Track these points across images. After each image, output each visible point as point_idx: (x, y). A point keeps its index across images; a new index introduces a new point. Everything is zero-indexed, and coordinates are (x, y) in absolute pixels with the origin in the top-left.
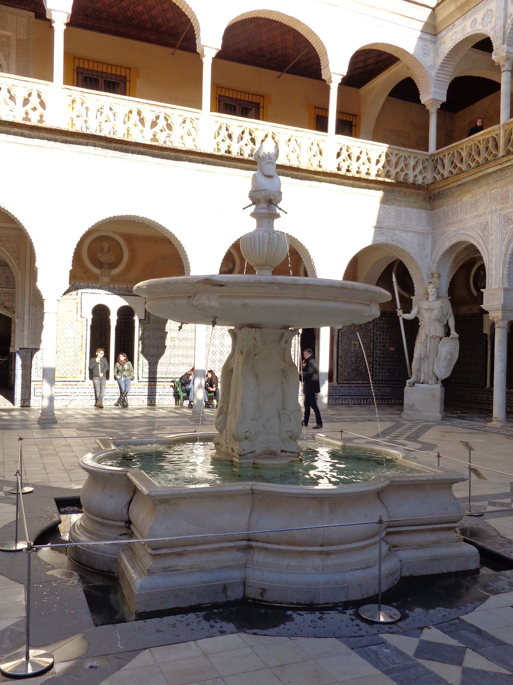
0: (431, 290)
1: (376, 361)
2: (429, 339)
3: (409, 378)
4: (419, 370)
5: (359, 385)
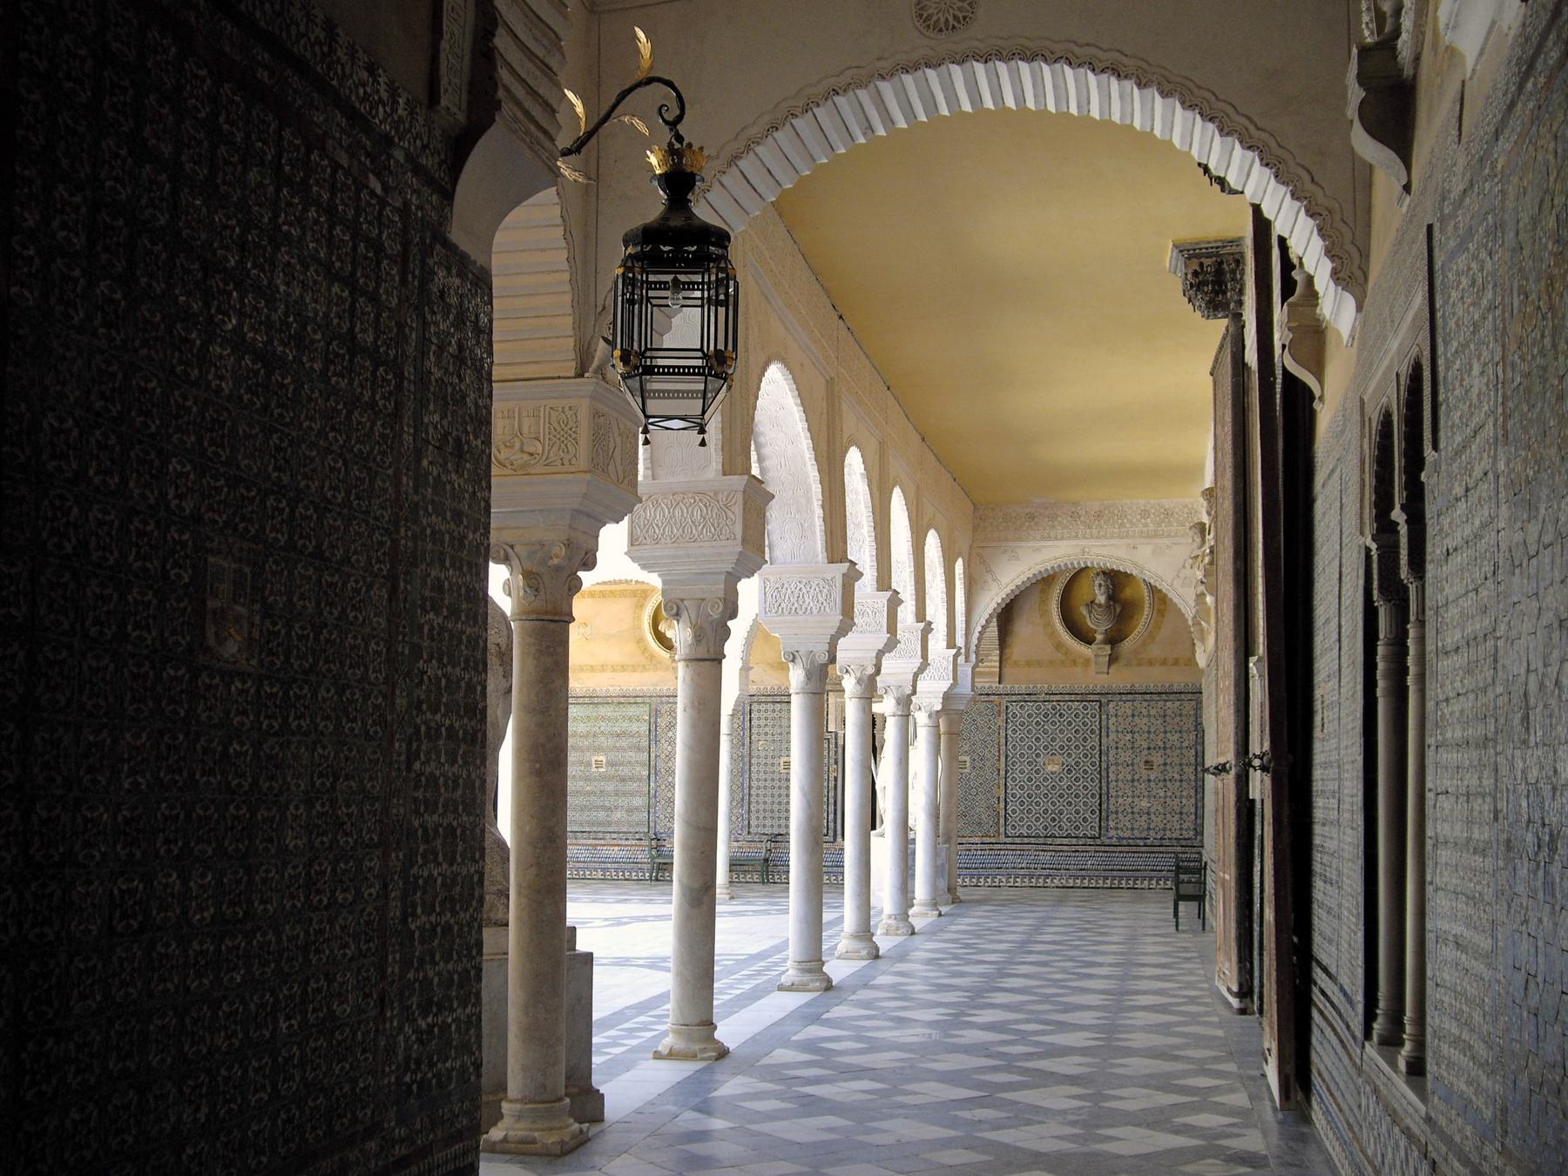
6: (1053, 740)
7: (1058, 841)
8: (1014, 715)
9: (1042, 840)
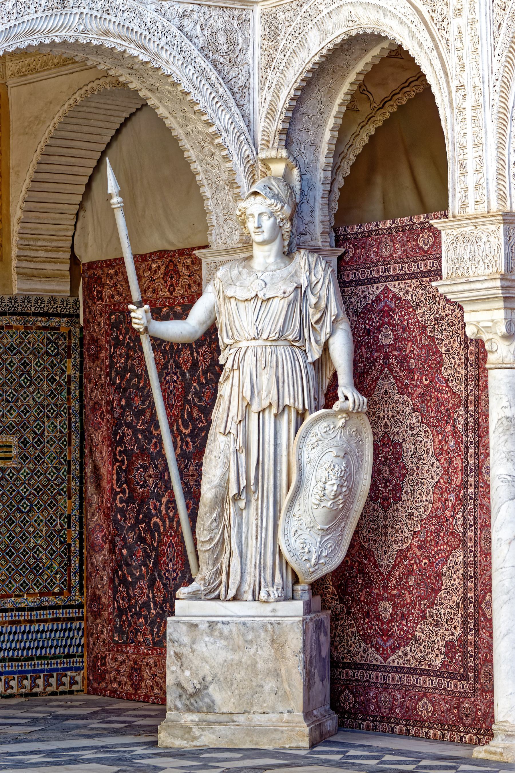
2: (254, 417)
5: (25, 616)
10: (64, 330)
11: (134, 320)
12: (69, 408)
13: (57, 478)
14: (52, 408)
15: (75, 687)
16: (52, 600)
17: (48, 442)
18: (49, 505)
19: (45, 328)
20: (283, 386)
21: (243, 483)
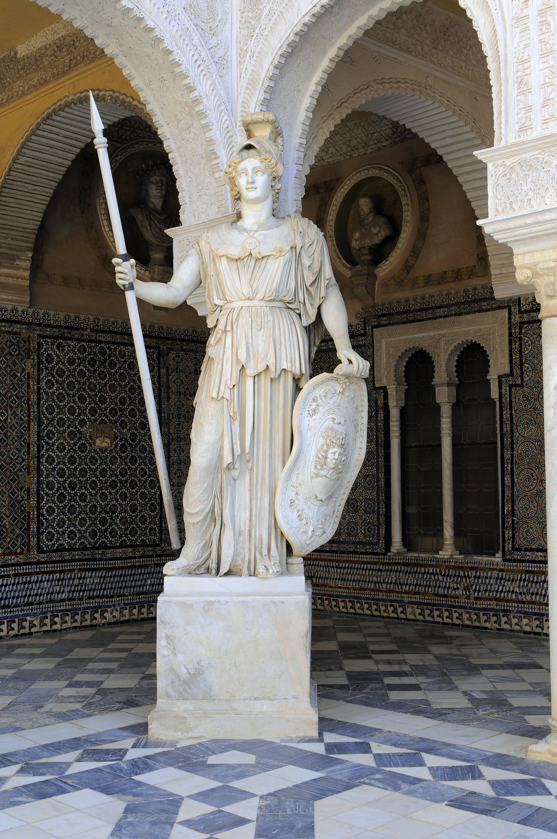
0: (253, 178)
1: (50, 486)
3: (175, 555)
4: (214, 517)
6: (103, 400)
7: (109, 553)
8: (50, 359)
9: (87, 554)
10: (24, 335)
11: (118, 275)
12: (29, 400)
13: (18, 457)
14: (14, 399)
15: (33, 630)
16: (13, 559)
17: (10, 428)
18: (11, 480)
19: (8, 332)
20: (280, 349)
21: (237, 451)
